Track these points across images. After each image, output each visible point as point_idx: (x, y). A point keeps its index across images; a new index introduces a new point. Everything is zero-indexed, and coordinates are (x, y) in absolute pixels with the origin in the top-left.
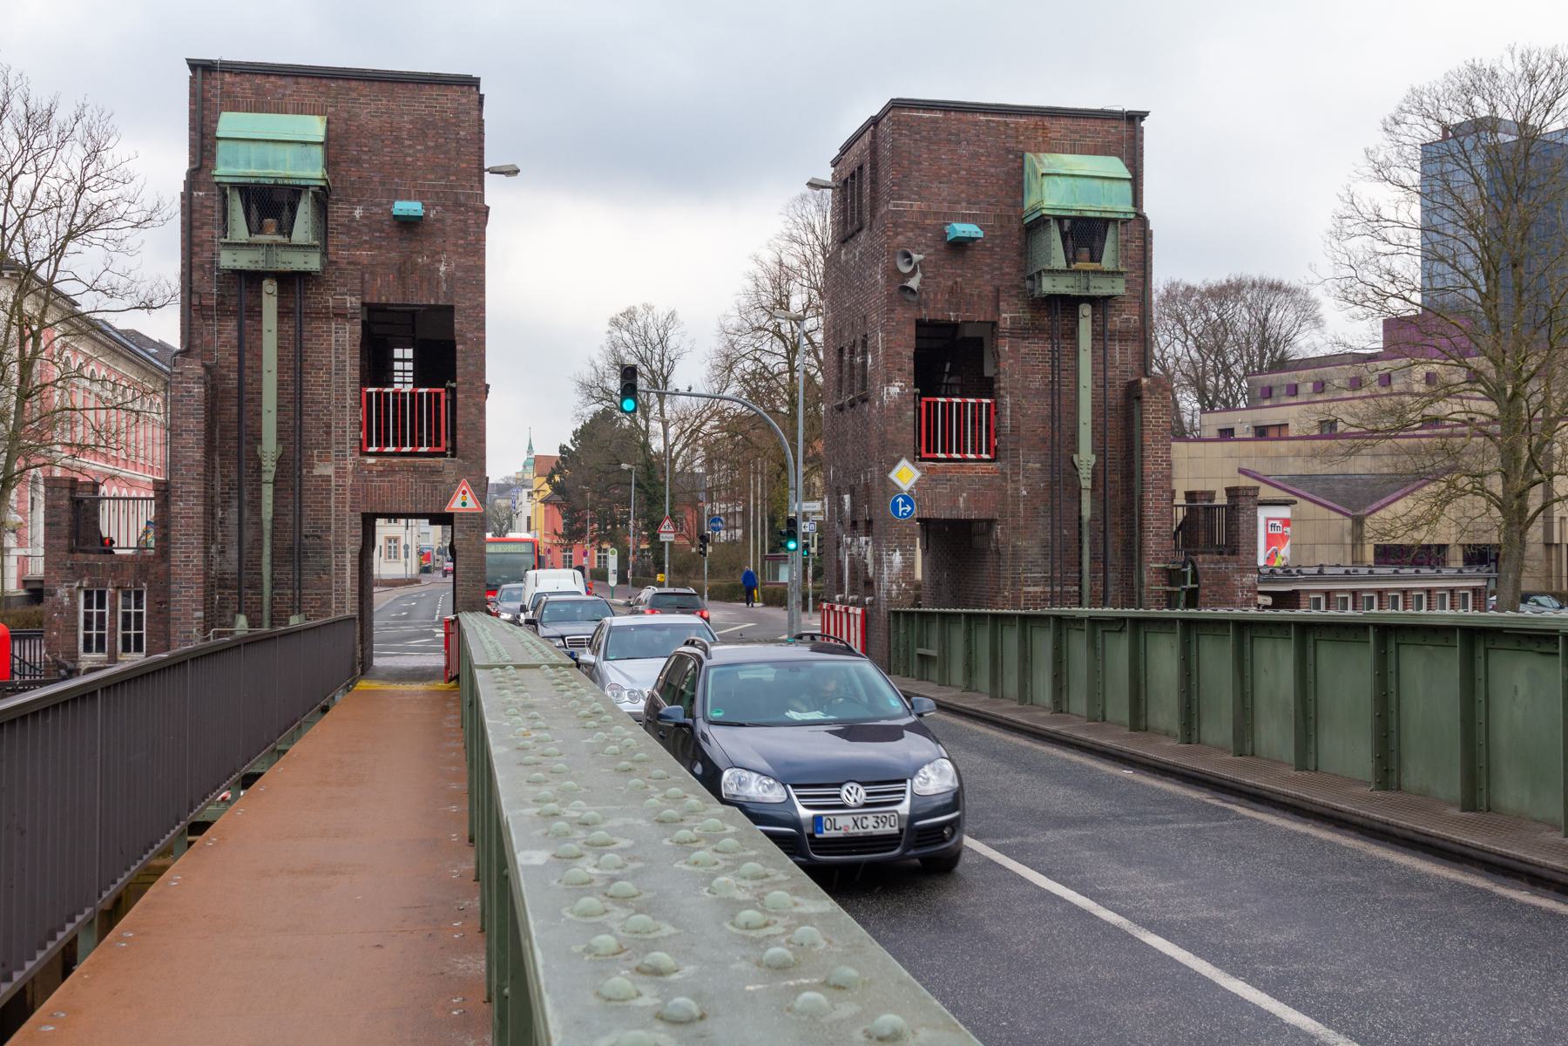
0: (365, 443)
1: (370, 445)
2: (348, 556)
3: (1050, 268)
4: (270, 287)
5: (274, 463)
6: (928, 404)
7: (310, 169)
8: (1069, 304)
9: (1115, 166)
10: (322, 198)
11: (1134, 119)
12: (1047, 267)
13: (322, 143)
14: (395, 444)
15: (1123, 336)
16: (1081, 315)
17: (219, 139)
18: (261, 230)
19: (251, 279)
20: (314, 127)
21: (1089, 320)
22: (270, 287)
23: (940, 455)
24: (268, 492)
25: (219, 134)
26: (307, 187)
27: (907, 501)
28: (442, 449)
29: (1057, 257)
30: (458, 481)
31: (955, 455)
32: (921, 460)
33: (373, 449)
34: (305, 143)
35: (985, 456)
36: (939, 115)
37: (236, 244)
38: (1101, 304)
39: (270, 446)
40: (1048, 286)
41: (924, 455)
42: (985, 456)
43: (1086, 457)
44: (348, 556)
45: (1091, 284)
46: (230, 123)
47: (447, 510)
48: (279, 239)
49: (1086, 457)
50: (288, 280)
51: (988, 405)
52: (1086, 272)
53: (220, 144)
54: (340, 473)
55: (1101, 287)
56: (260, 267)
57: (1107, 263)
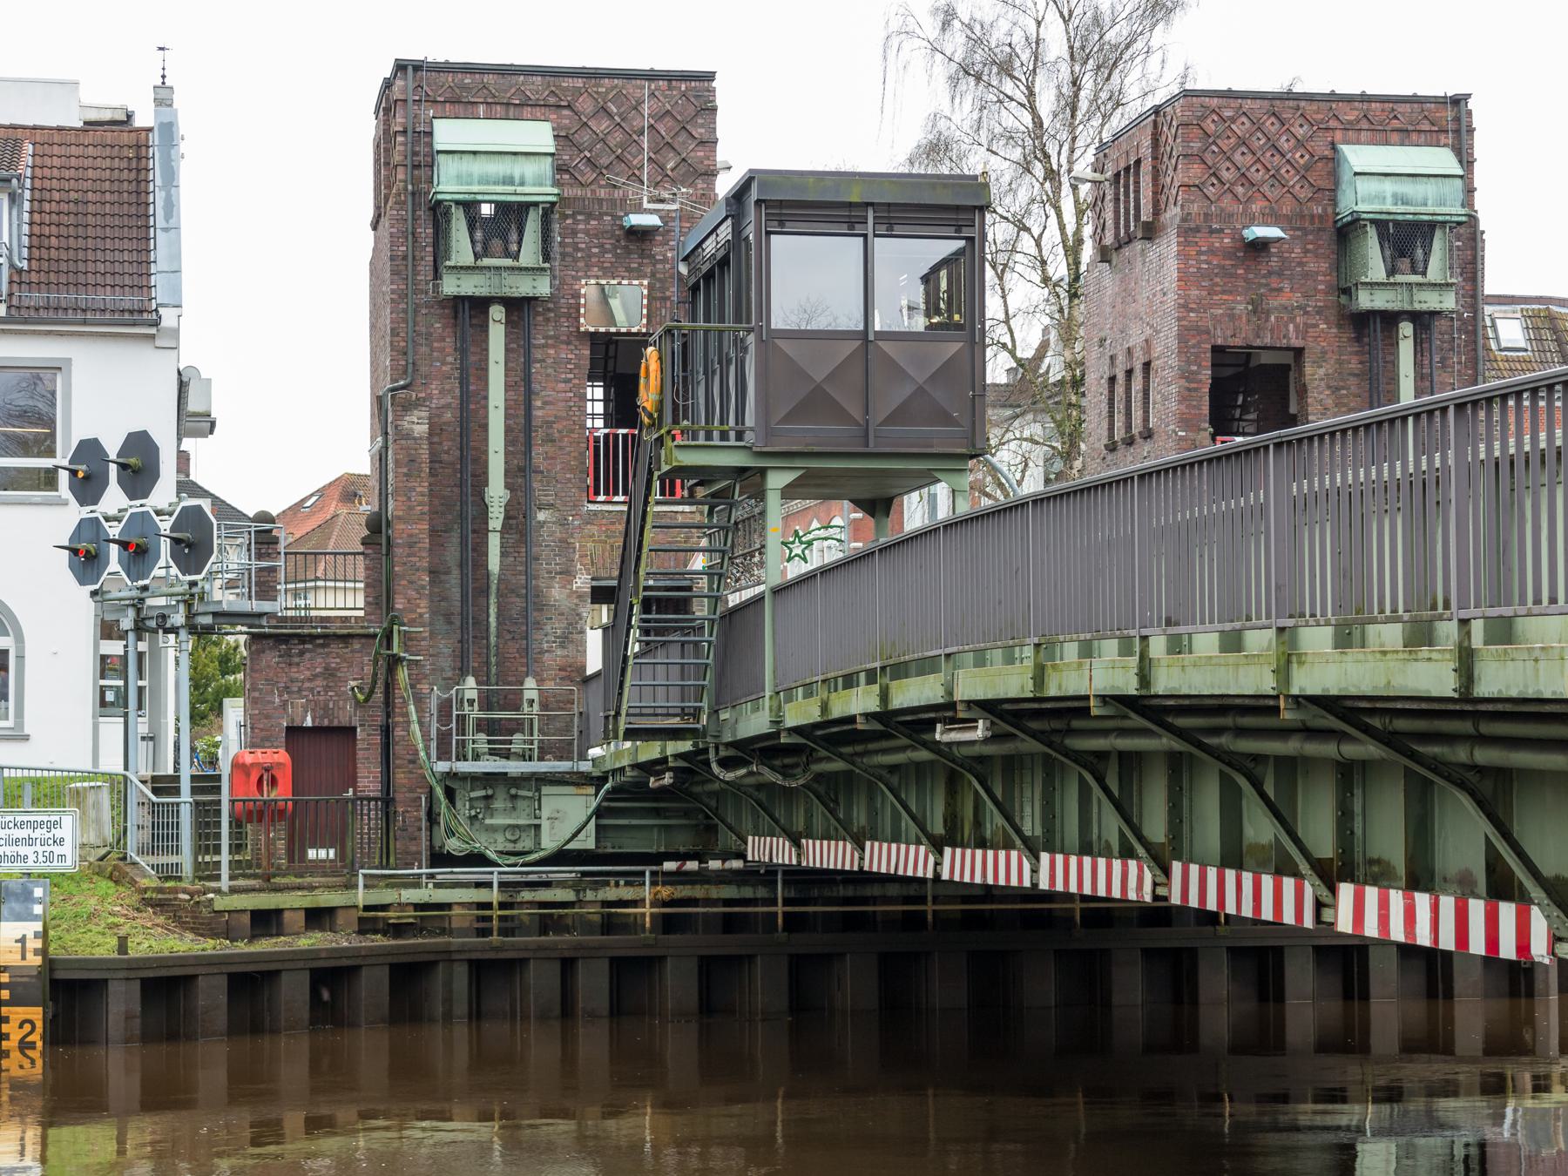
0: (592, 490)
3: (1368, 280)
4: (497, 313)
5: (502, 510)
7: (536, 183)
8: (1390, 319)
9: (1441, 159)
10: (548, 211)
12: (1363, 279)
13: (552, 155)
16: (1401, 336)
18: (486, 252)
19: (480, 305)
20: (538, 135)
21: (1410, 342)
22: (497, 313)
24: (494, 542)
25: (438, 147)
26: (536, 204)
29: (1376, 268)
33: (602, 498)
37: (461, 267)
38: (1423, 320)
39: (497, 491)
40: (1366, 301)
45: (1415, 298)
46: (449, 133)
48: (508, 262)
50: (518, 307)
55: (1429, 301)
56: (483, 291)
57: (1435, 271)
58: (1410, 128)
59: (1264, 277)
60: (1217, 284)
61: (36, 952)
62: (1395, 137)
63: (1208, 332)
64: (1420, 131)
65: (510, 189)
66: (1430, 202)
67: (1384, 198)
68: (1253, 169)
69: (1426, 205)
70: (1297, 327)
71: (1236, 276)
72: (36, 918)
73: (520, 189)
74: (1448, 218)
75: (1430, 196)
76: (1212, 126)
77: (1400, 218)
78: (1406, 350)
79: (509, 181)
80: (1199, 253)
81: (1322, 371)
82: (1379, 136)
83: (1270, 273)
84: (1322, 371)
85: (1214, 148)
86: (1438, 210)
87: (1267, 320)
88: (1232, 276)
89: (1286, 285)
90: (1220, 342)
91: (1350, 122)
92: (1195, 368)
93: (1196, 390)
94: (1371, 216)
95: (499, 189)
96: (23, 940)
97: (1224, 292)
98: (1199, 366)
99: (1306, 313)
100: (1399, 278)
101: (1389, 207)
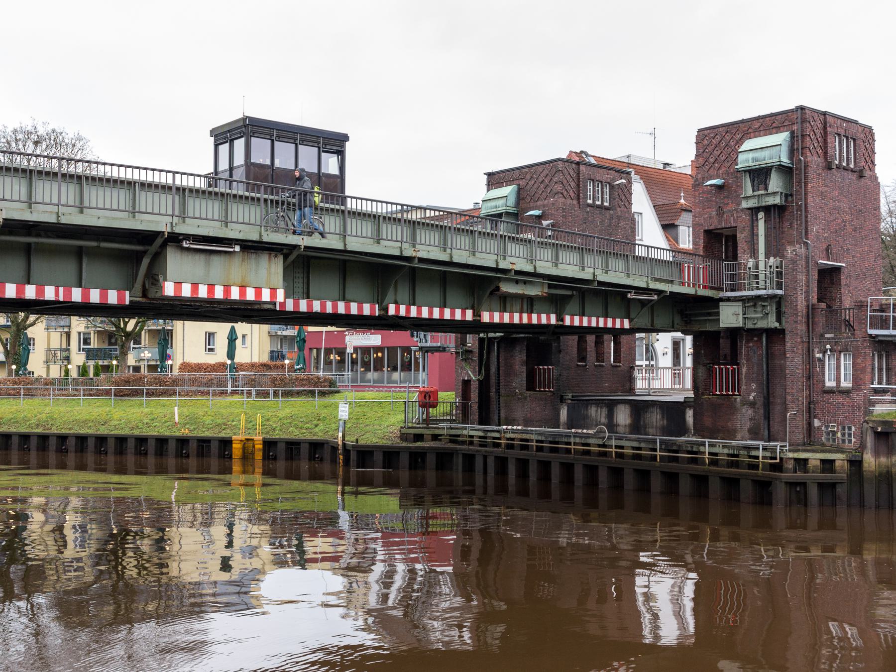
21: (763, 220)
58: (780, 125)
59: (722, 199)
60: (705, 205)
62: (774, 130)
63: (702, 225)
64: (784, 126)
65: (495, 210)
66: (766, 159)
67: (749, 161)
68: (721, 156)
69: (765, 160)
70: (734, 218)
71: (711, 201)
73: (498, 209)
74: (772, 164)
75: (766, 156)
76: (706, 142)
77: (754, 167)
79: (496, 207)
80: (699, 194)
81: (743, 235)
82: (768, 132)
83: (724, 197)
84: (743, 235)
85: (707, 150)
86: (768, 162)
87: (722, 217)
88: (711, 201)
89: (730, 202)
90: (706, 228)
91: (756, 129)
92: (698, 240)
93: (698, 248)
94: (743, 169)
95: (493, 210)
97: (708, 208)
98: (699, 239)
99: (737, 212)
101: (750, 164)
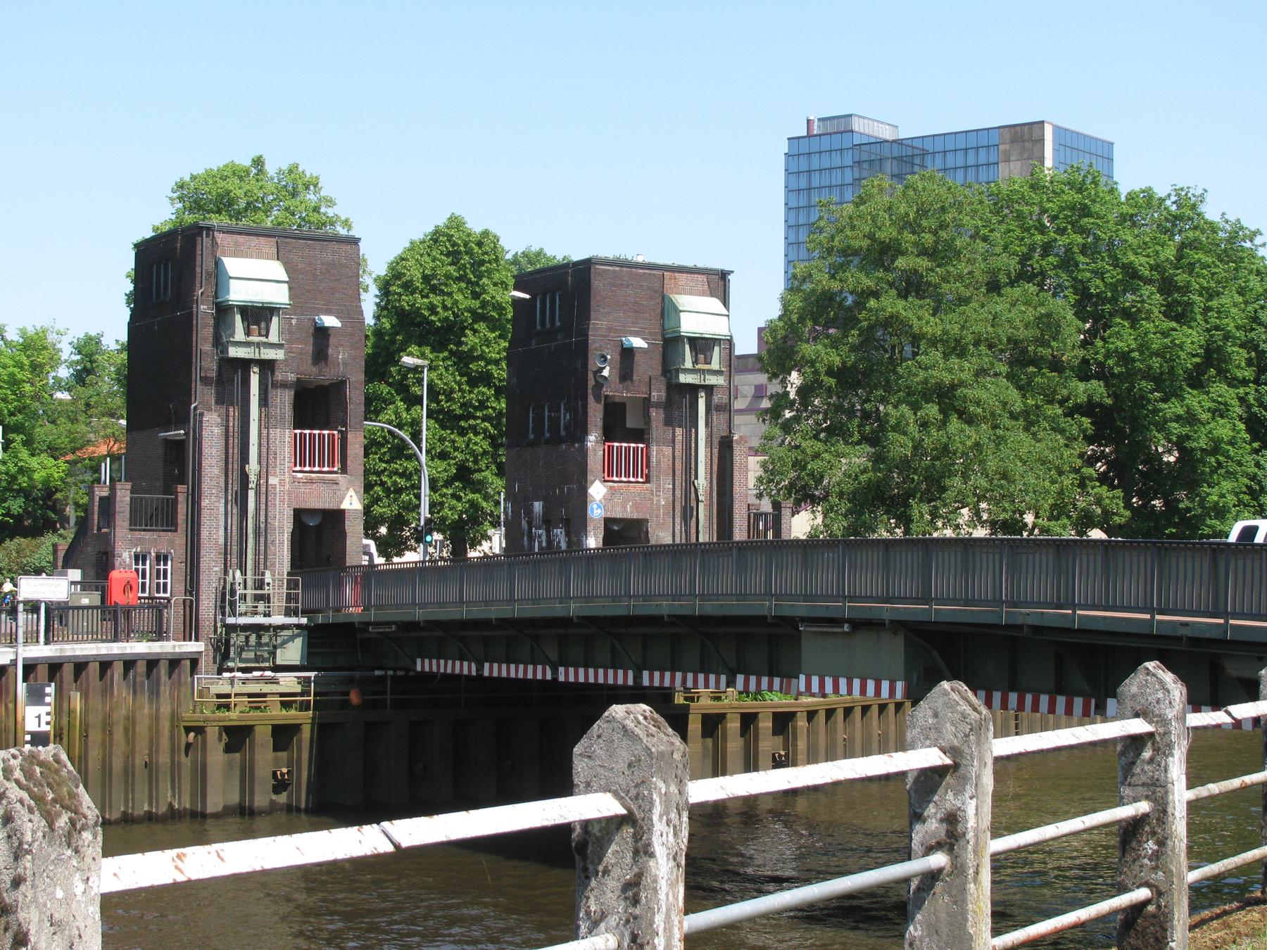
1: (295, 466)
2: (286, 535)
6: (609, 447)
7: (279, 295)
11: (724, 275)
14: (310, 466)
15: (720, 408)
17: (231, 278)
23: (615, 478)
27: (599, 507)
28: (336, 469)
30: (348, 489)
31: (624, 479)
32: (605, 481)
34: (278, 282)
35: (640, 479)
36: (617, 269)
38: (709, 389)
41: (607, 478)
42: (640, 479)
43: (702, 482)
44: (286, 535)
47: (343, 507)
48: (263, 339)
49: (702, 482)
50: (267, 366)
51: (642, 449)
52: (704, 370)
53: (232, 281)
54: (282, 482)
55: (712, 380)
61: (48, 723)
72: (49, 704)
78: (702, 403)
96: (39, 717)
100: (251, 339)
